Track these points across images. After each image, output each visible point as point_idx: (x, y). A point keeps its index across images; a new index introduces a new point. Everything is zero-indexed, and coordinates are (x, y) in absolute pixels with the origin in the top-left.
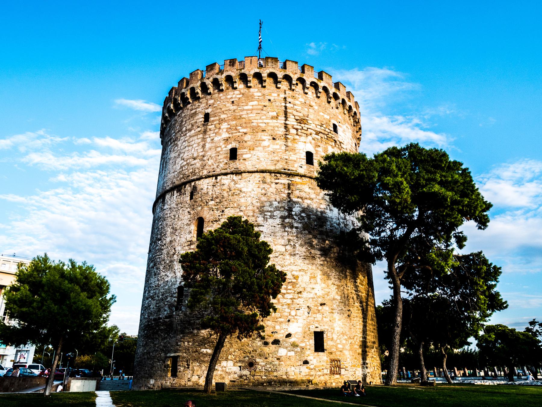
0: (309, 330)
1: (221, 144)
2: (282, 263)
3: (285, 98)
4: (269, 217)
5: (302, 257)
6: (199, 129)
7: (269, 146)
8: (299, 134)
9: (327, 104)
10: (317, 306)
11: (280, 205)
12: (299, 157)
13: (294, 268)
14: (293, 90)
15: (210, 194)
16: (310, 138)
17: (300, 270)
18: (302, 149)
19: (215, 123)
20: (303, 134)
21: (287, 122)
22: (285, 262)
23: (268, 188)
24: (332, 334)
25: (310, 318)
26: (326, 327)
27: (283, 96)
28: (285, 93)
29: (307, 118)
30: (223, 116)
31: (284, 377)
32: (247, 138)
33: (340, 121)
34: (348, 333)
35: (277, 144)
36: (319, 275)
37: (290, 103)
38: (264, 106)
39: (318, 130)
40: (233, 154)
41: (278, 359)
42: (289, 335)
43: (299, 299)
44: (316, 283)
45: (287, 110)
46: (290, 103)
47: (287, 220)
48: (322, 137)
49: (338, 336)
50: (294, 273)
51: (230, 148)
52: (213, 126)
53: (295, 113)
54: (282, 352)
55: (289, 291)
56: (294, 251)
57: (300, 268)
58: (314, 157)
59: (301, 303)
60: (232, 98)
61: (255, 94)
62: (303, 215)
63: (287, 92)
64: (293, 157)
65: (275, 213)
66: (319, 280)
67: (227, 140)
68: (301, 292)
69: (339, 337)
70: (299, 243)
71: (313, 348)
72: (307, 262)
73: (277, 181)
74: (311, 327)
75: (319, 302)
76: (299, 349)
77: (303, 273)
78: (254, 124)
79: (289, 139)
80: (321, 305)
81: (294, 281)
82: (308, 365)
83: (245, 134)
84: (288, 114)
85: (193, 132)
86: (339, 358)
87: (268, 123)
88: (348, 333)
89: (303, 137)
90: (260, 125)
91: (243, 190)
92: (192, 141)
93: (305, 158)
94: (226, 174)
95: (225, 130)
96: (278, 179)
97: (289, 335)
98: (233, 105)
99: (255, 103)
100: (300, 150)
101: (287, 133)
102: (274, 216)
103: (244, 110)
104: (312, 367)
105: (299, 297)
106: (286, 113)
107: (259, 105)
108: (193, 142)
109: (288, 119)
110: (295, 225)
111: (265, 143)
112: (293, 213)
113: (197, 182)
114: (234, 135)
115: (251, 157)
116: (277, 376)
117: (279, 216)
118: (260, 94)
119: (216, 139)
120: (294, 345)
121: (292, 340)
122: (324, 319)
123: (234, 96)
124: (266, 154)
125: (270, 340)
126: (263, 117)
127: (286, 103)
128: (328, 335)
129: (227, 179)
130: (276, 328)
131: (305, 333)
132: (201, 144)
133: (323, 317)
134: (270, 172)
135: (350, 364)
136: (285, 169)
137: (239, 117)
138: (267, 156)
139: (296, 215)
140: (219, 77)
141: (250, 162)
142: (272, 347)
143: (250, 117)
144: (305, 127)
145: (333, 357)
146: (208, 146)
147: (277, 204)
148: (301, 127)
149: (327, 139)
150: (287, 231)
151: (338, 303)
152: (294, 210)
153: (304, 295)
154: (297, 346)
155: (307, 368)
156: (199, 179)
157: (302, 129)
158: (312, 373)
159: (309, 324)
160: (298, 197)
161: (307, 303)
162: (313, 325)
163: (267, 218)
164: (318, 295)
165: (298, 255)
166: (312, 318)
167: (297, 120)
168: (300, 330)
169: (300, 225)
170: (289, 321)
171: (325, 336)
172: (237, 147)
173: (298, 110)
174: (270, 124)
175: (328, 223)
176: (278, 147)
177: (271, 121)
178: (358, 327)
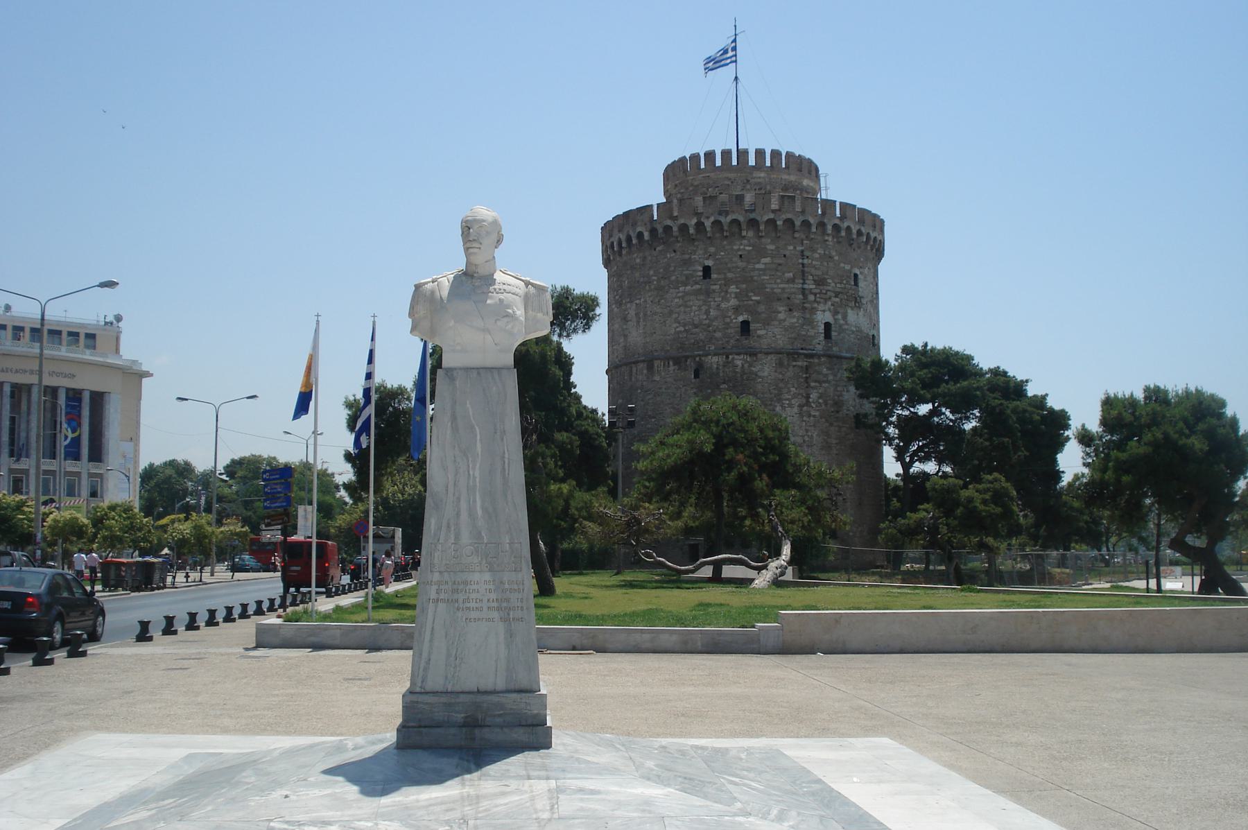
1: (730, 314)
3: (802, 251)
6: (698, 287)
7: (785, 320)
11: (797, 392)
12: (816, 331)
14: (812, 239)
15: (721, 375)
19: (719, 282)
20: (822, 300)
21: (806, 286)
23: (786, 372)
27: (799, 248)
28: (802, 244)
30: (730, 275)
32: (762, 308)
35: (794, 317)
38: (780, 265)
39: (838, 290)
40: (745, 327)
46: (807, 257)
47: (805, 408)
48: (841, 300)
51: (741, 320)
52: (718, 287)
53: (813, 271)
58: (833, 329)
60: (739, 250)
61: (768, 247)
62: (820, 401)
63: (805, 242)
64: (812, 333)
65: (793, 402)
67: (737, 310)
72: (823, 452)
73: (794, 363)
78: (768, 290)
83: (758, 302)
84: (806, 275)
85: (688, 288)
87: (783, 289)
90: (775, 290)
91: (760, 374)
92: (690, 300)
93: (823, 331)
94: (739, 354)
95: (733, 296)
96: (796, 361)
98: (742, 261)
99: (767, 260)
101: (805, 301)
103: (754, 269)
106: (803, 272)
107: (772, 263)
108: (691, 303)
110: (813, 413)
111: (781, 316)
112: (811, 400)
113: (703, 358)
114: (746, 303)
115: (767, 334)
117: (797, 404)
118: (772, 247)
119: (723, 305)
123: (742, 247)
124: (781, 330)
126: (779, 281)
127: (803, 259)
129: (740, 360)
132: (704, 308)
134: (788, 354)
136: (802, 349)
137: (750, 279)
138: (783, 333)
139: (813, 402)
140: (722, 219)
141: (765, 340)
143: (764, 280)
146: (713, 313)
147: (795, 391)
150: (805, 421)
152: (811, 396)
156: (706, 355)
160: (816, 381)
169: (817, 414)
172: (750, 320)
174: (786, 291)
175: (845, 408)
176: (795, 320)
177: (786, 286)
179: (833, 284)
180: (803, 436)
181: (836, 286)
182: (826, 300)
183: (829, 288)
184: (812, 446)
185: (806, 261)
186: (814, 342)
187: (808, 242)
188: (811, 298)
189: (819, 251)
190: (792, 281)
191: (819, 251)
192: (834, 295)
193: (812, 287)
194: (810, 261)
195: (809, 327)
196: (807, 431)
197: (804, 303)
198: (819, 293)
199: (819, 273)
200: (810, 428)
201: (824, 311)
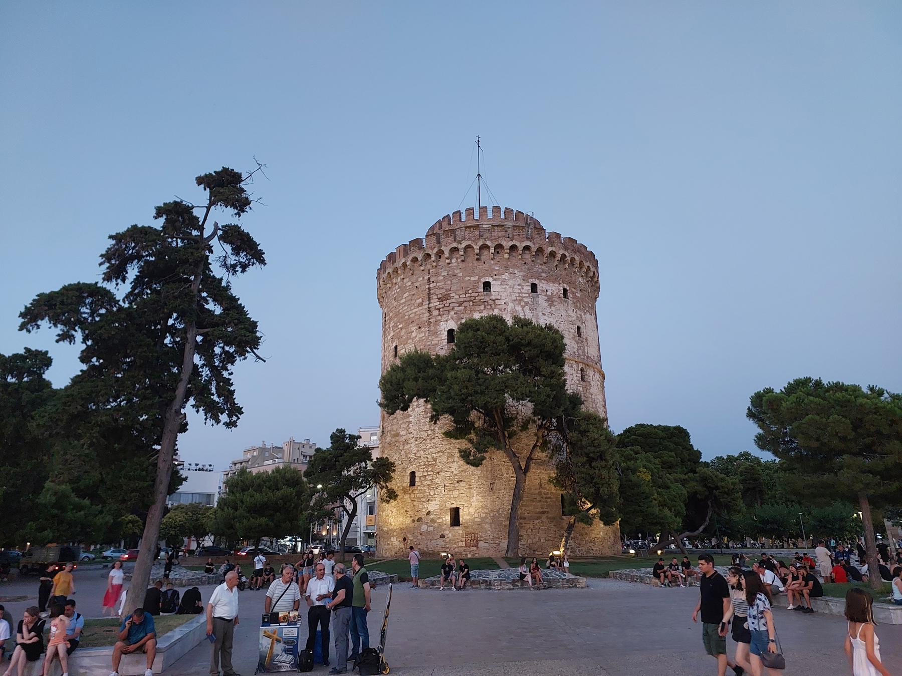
9: (476, 263)
12: (440, 339)
13: (433, 450)
16: (452, 313)
17: (438, 452)
29: (449, 292)
33: (495, 273)
37: (433, 282)
45: (431, 291)
46: (433, 282)
48: (465, 307)
53: (438, 292)
55: (429, 473)
68: (439, 472)
89: (444, 316)
105: (438, 478)
109: (431, 301)
144: (447, 303)
149: (473, 305)
164: (455, 472)
167: (439, 299)
179: (457, 297)
183: (453, 300)
186: (437, 349)
188: (435, 313)
189: (442, 274)
190: (421, 305)
191: (442, 274)
193: (435, 304)
195: (433, 337)
197: (429, 319)
198: (443, 308)
199: (443, 291)
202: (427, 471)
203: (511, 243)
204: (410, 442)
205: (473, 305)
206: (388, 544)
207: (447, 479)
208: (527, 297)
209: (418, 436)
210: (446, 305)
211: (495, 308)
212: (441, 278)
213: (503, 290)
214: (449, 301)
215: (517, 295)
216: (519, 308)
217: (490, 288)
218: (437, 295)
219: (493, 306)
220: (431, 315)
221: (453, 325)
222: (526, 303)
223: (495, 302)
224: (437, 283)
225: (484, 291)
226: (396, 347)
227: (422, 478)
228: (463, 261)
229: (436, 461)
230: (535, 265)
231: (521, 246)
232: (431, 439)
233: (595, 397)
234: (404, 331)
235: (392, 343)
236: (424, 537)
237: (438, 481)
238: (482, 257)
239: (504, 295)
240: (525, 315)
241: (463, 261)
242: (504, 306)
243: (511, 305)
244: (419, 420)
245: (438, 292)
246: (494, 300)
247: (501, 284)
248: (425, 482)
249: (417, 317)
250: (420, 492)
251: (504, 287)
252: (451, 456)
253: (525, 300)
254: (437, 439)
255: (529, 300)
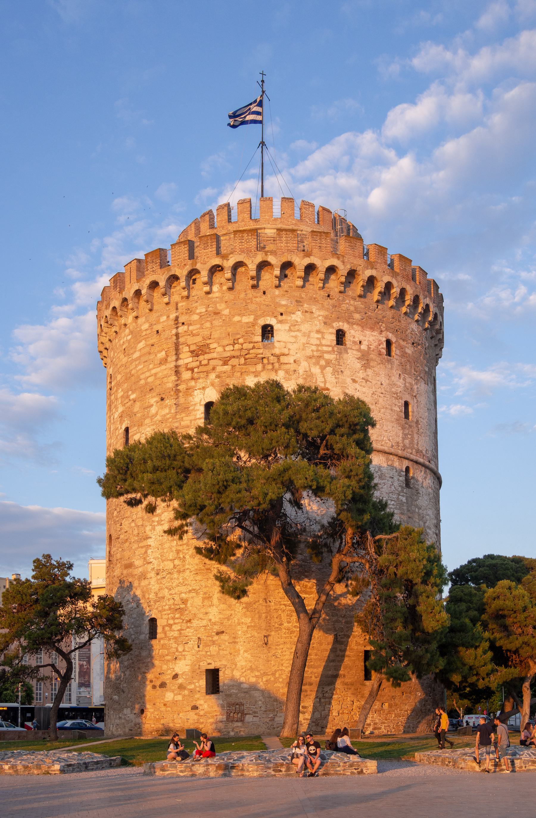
0: (199, 668)
2: (170, 584)
3: (177, 318)
4: (156, 523)
5: (193, 573)
8: (196, 375)
10: (212, 636)
13: (183, 589)
16: (212, 376)
17: (190, 591)
18: (199, 402)
22: (172, 583)
24: (233, 670)
25: (200, 653)
26: (224, 662)
27: (173, 316)
28: (177, 309)
31: (171, 725)
34: (261, 667)
36: (216, 593)
37: (183, 324)
41: (165, 705)
42: (176, 676)
43: (188, 630)
44: (212, 605)
45: (181, 340)
46: (183, 324)
48: (233, 366)
49: (243, 673)
50: (183, 595)
53: (191, 340)
54: (169, 696)
55: (177, 621)
56: (184, 566)
57: (190, 589)
59: (190, 634)
63: (180, 305)
66: (215, 601)
69: (244, 674)
70: (190, 553)
71: (204, 690)
72: (199, 578)
74: (201, 664)
75: (215, 630)
76: (186, 692)
77: (194, 594)
79: (181, 392)
80: (218, 633)
81: (182, 606)
82: (197, 711)
84: (181, 347)
86: (242, 701)
88: (261, 667)
89: (200, 381)
93: (203, 415)
97: (176, 676)
100: (195, 405)
102: (162, 521)
104: (202, 713)
105: (188, 627)
109: (181, 356)
116: (163, 724)
117: (167, 520)
120: (181, 687)
121: (180, 681)
122: (221, 652)
125: (158, 683)
128: (226, 672)
130: (163, 669)
131: (193, 672)
133: (219, 650)
135: (263, 709)
142: (159, 690)
145: (232, 700)
148: (198, 363)
149: (245, 364)
151: (245, 628)
153: (195, 623)
154: (185, 688)
155: (196, 714)
157: (201, 365)
158: (201, 720)
159: (199, 660)
161: (198, 634)
162: (205, 662)
163: (154, 526)
164: (213, 620)
165: (188, 571)
166: (204, 653)
167: (192, 352)
168: (187, 669)
170: (176, 658)
171: (221, 674)
173: (194, 332)
178: (287, 657)
179: (220, 349)
180: (172, 560)
181: (225, 350)
182: (208, 372)
183: (214, 355)
184: (184, 571)
185: (182, 329)
187: (184, 304)
188: (187, 375)
189: (198, 311)
192: (221, 363)
193: (186, 361)
194: (185, 328)
195: (183, 415)
196: (178, 552)
197: (177, 385)
198: (198, 367)
199: (198, 339)
200: (180, 548)
201: (204, 388)
202: (174, 618)
203: (307, 261)
204: (149, 577)
205: (245, 364)
206: (120, 718)
207: (202, 629)
208: (328, 352)
209: (161, 567)
210: (203, 363)
211: (280, 369)
212: (196, 317)
213: (292, 340)
214: (207, 356)
215: (314, 348)
216: (316, 370)
217: (272, 336)
218: (189, 346)
219: (277, 365)
220: (179, 378)
221: (213, 395)
222: (328, 363)
223: (279, 359)
224: (190, 325)
225: (262, 341)
226: (127, 430)
227: (167, 628)
228: (231, 289)
229: (186, 604)
230: (344, 300)
231: (322, 265)
232: (179, 572)
233: (425, 512)
234: (138, 404)
235: (121, 423)
236: (169, 709)
237: (189, 632)
238: (261, 283)
239: (293, 347)
240: (325, 382)
241: (231, 289)
242: (292, 367)
243: (304, 365)
244: (162, 545)
245: (191, 340)
246: (278, 357)
247: (290, 330)
248: (171, 634)
249: (158, 382)
250: (163, 647)
251: (293, 334)
252: (208, 597)
253: (327, 356)
254: (187, 572)
255: (332, 357)
